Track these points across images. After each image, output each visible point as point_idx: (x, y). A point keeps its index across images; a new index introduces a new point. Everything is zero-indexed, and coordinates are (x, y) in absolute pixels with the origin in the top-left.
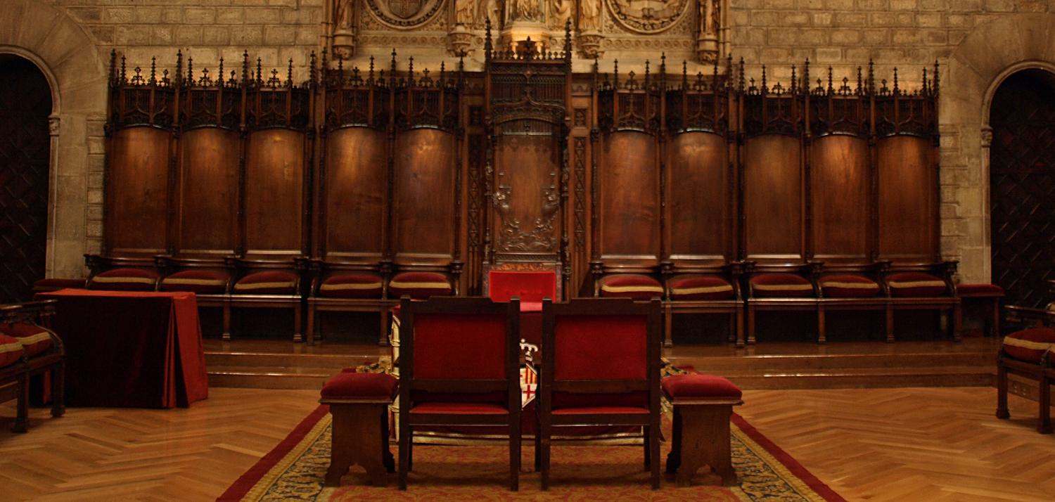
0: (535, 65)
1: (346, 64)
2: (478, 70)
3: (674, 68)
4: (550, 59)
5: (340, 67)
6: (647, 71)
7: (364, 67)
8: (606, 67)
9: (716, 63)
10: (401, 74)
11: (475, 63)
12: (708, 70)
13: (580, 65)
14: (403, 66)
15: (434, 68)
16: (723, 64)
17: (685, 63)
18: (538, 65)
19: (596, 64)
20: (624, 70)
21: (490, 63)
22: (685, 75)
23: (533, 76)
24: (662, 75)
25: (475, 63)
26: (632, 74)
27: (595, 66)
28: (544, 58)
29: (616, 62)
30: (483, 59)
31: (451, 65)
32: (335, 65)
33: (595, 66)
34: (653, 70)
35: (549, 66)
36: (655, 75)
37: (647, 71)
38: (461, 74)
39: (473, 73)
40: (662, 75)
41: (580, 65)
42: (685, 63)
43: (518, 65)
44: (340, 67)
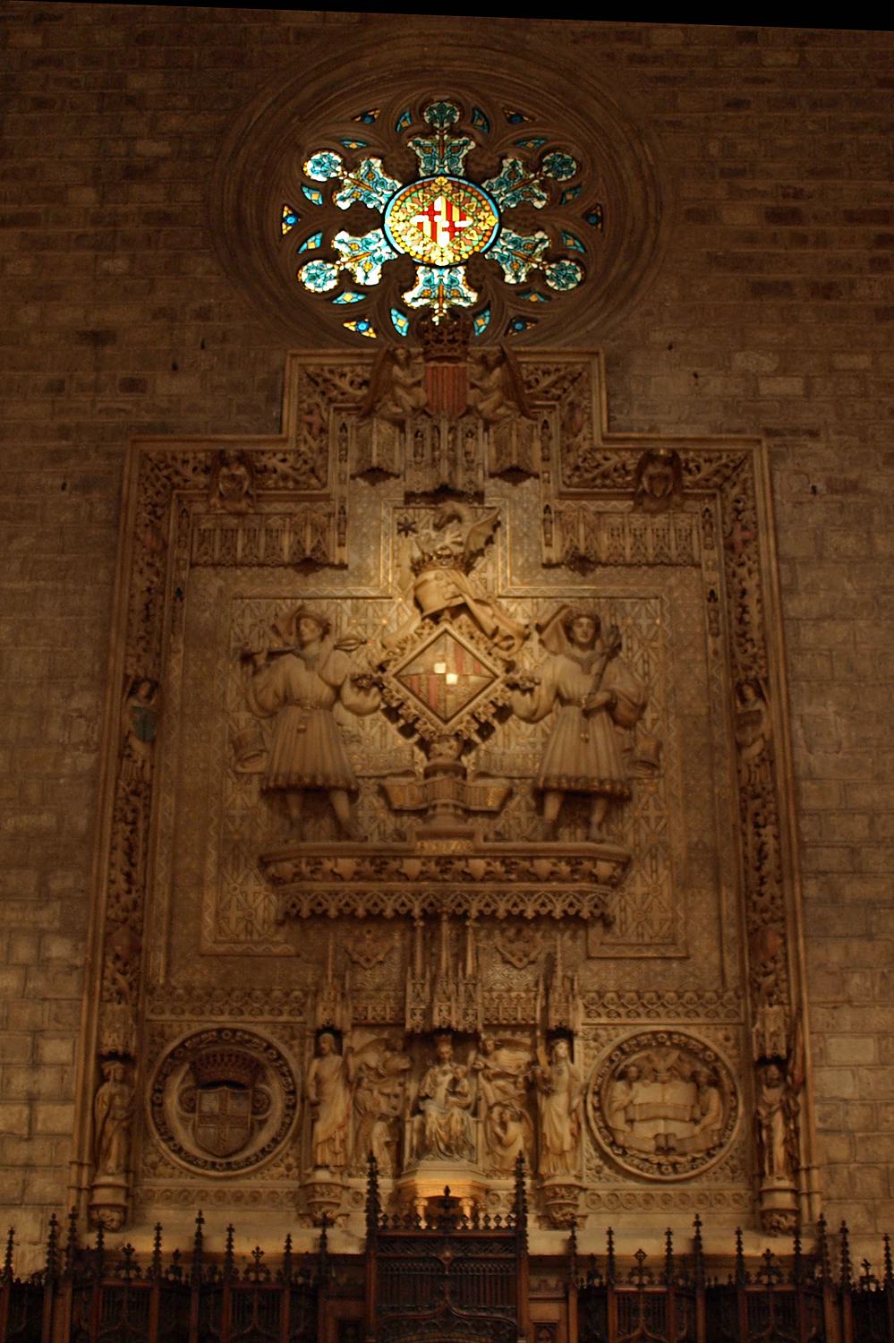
0: (460, 1240)
1: (111, 1240)
2: (353, 1250)
3: (719, 1243)
4: (487, 1228)
5: (100, 1243)
6: (669, 1250)
7: (143, 1244)
8: (591, 1244)
9: (796, 1232)
10: (213, 1258)
11: (348, 1239)
12: (782, 1246)
13: (543, 1241)
14: (216, 1245)
15: (273, 1247)
16: (809, 1235)
17: (739, 1233)
18: (464, 1241)
19: (573, 1238)
20: (625, 1248)
21: (376, 1236)
22: (740, 1256)
23: (456, 1260)
24: (697, 1257)
25: (348, 1239)
26: (640, 1255)
27: (572, 1243)
28: (476, 1227)
29: (610, 1233)
30: (360, 1229)
31: (304, 1241)
32: (90, 1240)
33: (572, 1243)
34: (680, 1247)
35: (484, 1241)
36: (683, 1258)
37: (669, 1250)
38: (323, 1258)
39: (345, 1256)
40: (697, 1257)
41: (543, 1241)
42: (739, 1233)
43: (429, 1241)
44: (100, 1243)
